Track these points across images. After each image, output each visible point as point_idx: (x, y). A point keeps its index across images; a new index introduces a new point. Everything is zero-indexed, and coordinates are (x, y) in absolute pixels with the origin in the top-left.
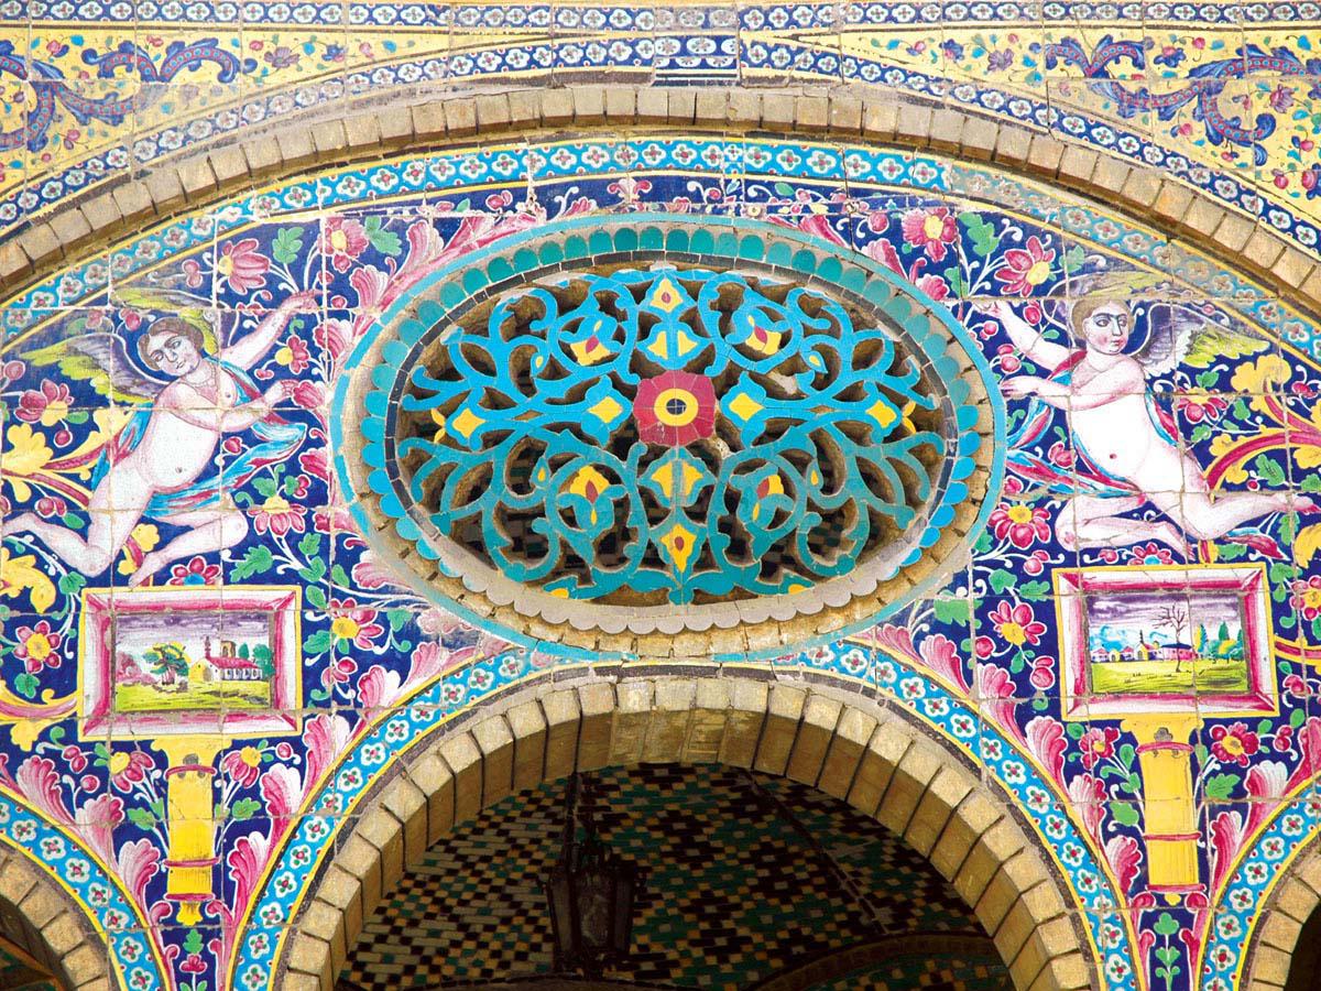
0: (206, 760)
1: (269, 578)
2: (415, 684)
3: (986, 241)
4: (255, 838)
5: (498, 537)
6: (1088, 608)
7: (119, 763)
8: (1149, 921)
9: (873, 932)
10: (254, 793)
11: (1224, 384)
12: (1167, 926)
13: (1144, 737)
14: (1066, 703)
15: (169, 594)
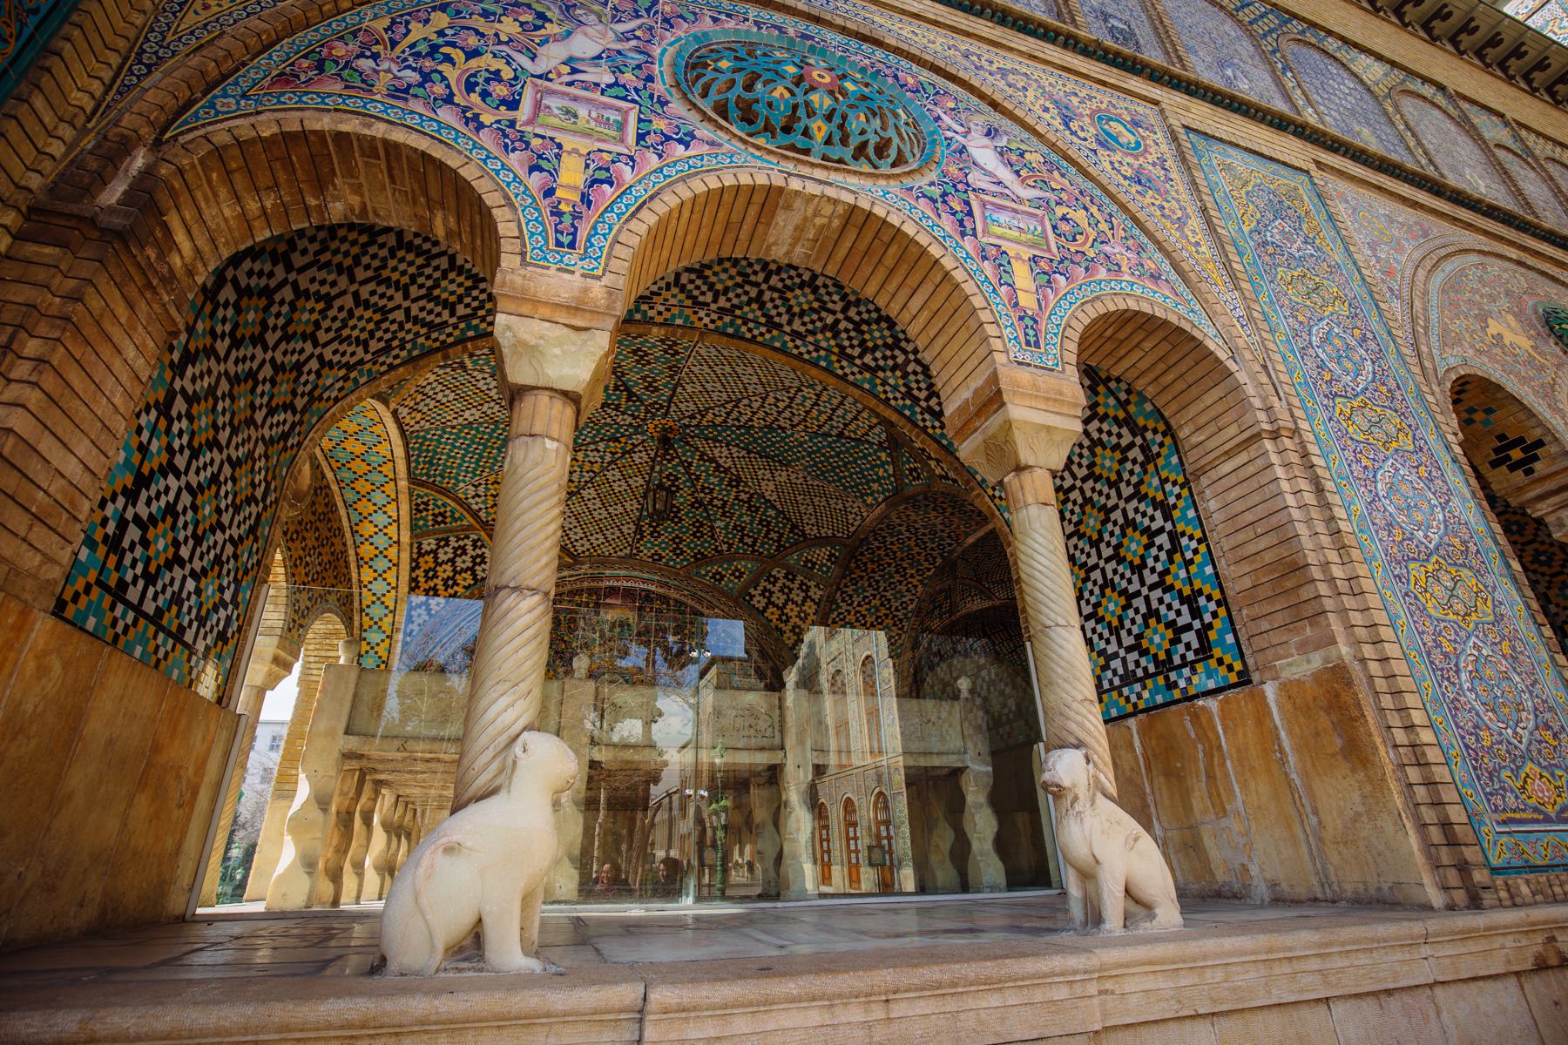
0: (585, 152)
1: (624, 99)
2: (689, 153)
3: (931, 90)
4: (605, 187)
5: (734, 113)
6: (984, 204)
7: (536, 142)
8: (1021, 318)
9: (720, 552)
10: (608, 170)
11: (1022, 155)
12: (1030, 323)
13: (1011, 254)
14: (979, 235)
15: (572, 90)
